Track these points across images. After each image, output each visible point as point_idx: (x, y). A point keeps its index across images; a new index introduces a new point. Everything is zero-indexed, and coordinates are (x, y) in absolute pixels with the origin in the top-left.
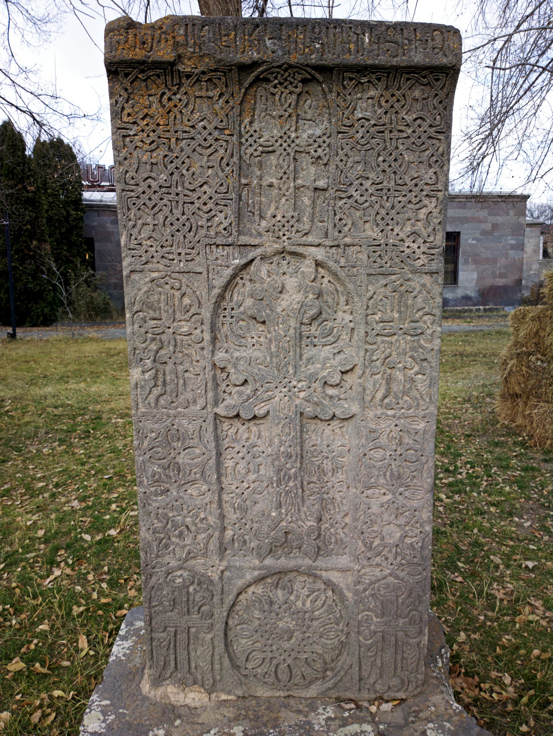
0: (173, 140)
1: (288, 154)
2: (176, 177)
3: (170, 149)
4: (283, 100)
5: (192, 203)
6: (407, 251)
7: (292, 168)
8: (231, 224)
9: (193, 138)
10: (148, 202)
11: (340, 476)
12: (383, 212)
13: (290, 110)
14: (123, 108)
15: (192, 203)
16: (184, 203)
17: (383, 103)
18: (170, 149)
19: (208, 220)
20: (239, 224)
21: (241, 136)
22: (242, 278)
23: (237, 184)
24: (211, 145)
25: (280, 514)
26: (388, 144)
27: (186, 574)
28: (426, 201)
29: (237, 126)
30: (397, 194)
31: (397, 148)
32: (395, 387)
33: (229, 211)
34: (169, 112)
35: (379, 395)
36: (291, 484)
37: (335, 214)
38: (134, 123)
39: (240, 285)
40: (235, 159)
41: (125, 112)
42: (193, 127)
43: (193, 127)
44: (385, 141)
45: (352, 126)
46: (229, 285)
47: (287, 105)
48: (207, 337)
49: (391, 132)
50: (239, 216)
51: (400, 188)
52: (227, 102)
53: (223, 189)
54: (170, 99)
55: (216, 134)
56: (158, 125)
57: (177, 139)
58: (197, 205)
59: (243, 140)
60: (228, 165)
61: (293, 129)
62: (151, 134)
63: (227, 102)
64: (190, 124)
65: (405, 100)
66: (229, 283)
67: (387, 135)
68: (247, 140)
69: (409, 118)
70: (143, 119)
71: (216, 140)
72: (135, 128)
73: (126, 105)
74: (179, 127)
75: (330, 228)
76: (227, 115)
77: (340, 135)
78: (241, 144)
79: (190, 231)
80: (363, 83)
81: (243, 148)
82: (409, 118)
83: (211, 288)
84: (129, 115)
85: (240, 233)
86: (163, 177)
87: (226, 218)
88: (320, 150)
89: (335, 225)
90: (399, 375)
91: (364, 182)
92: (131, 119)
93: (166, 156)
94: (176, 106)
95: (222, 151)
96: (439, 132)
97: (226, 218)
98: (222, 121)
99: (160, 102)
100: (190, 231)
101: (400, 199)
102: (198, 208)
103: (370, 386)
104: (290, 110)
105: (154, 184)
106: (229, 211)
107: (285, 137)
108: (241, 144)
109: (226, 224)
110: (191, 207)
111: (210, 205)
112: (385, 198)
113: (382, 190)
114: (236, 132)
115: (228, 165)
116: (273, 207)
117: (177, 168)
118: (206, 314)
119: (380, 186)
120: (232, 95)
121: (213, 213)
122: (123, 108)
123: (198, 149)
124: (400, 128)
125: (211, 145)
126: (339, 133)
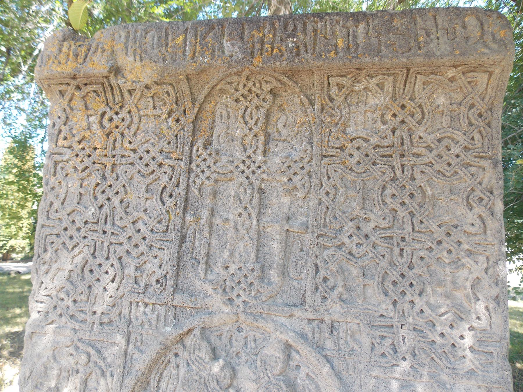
0: (109, 167)
1: (252, 183)
3: (104, 177)
4: (247, 118)
5: (121, 244)
6: (439, 340)
7: (255, 202)
8: (166, 275)
9: (132, 164)
10: (68, 242)
13: (256, 130)
14: (60, 131)
15: (121, 244)
16: (111, 243)
17: (388, 117)
18: (104, 177)
19: (137, 268)
20: (177, 275)
21: (191, 161)
22: (176, 355)
23: (179, 222)
24: (153, 172)
26: (399, 173)
28: (466, 260)
29: (187, 148)
30: (417, 246)
31: (413, 178)
34: (108, 135)
37: (317, 271)
38: (70, 147)
39: (173, 365)
40: (181, 190)
41: (62, 136)
42: (134, 150)
43: (134, 150)
44: (393, 168)
45: (342, 148)
49: (402, 156)
51: (419, 236)
52: (178, 120)
53: (162, 227)
54: (111, 120)
55: (160, 159)
56: (95, 149)
57: (113, 165)
58: (126, 247)
59: (193, 166)
60: (171, 196)
61: (259, 151)
62: (86, 160)
63: (178, 120)
64: (132, 147)
65: (423, 112)
66: (154, 362)
67: (396, 162)
68: (198, 166)
70: (79, 142)
71: (160, 165)
72: (69, 151)
73: (63, 128)
74: (118, 152)
75: (310, 289)
76: (176, 136)
77: (325, 160)
78: (190, 171)
79: (113, 281)
80: (358, 93)
81: (192, 176)
84: (65, 138)
85: (176, 288)
87: (160, 266)
88: (296, 179)
89: (317, 288)
91: (362, 225)
92: (66, 143)
93: (98, 184)
94: (117, 127)
95: (165, 179)
96: (481, 157)
97: (160, 266)
98: (169, 143)
99: (101, 123)
100: (113, 281)
101: (422, 253)
102: (128, 252)
104: (256, 130)
105: (77, 218)
107: (248, 162)
109: (159, 273)
110: (119, 249)
111: (142, 248)
112: (397, 251)
113: (392, 238)
114: (186, 155)
115: (171, 196)
116: (226, 254)
117: (109, 199)
119: (388, 233)
120: (185, 112)
121: (145, 258)
122: (60, 131)
124: (415, 150)
125: (153, 172)
126: (323, 156)
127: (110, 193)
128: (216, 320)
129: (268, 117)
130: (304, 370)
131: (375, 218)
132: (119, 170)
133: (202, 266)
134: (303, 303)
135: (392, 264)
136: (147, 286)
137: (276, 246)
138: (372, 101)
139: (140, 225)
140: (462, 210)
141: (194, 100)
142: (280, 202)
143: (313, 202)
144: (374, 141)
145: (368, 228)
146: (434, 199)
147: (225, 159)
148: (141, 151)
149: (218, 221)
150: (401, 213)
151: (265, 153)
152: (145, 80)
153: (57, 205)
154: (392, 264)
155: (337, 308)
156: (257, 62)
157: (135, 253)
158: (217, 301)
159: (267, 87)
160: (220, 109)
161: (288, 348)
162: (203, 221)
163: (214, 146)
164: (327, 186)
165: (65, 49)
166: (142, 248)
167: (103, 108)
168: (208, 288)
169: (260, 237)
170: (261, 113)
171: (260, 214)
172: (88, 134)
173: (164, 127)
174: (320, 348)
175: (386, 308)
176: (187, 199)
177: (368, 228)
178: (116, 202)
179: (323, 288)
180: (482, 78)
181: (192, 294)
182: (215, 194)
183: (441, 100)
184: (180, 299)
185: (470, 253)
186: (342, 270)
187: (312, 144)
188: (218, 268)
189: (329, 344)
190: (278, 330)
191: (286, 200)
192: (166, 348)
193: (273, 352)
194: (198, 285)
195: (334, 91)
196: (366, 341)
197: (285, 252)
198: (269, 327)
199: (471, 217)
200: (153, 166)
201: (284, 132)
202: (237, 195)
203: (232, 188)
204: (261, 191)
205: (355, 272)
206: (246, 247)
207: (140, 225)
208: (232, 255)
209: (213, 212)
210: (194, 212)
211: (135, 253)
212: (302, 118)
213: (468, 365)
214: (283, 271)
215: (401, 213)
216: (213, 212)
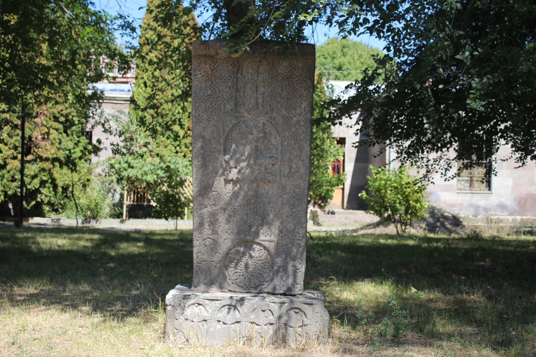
2: (214, 91)
3: (212, 83)
11: (271, 205)
12: (288, 106)
18: (212, 83)
21: (237, 79)
25: (247, 217)
27: (210, 240)
28: (304, 103)
32: (292, 170)
33: (232, 103)
34: (212, 70)
35: (286, 173)
36: (252, 207)
40: (235, 86)
46: (231, 130)
47: (254, 69)
48: (222, 148)
50: (236, 105)
54: (213, 66)
66: (231, 130)
69: (297, 74)
72: (200, 75)
78: (237, 81)
82: (297, 74)
83: (224, 131)
85: (236, 112)
86: (209, 92)
90: (294, 166)
103: (283, 169)
105: (205, 94)
106: (232, 103)
108: (237, 81)
109: (231, 108)
111: (225, 102)
118: (222, 140)
123: (222, 83)
127: (215, 87)
128: (246, 119)
129: (258, 67)
130: (268, 129)
131: (284, 94)
132: (217, 81)
133: (242, 106)
134: (267, 113)
135: (288, 104)
136: (227, 112)
137: (260, 101)
138: (284, 64)
139: (224, 96)
140: (303, 91)
141: (238, 62)
142: (262, 90)
143: (269, 90)
144: (285, 74)
145: (282, 96)
146: (298, 89)
147: (246, 78)
148: (223, 76)
149: (245, 95)
150: (290, 92)
151: (257, 77)
152: (225, 56)
153: (198, 91)
154: (288, 104)
155: (275, 114)
156: (256, 55)
157: (223, 103)
158: (246, 114)
159: (258, 60)
160: (245, 65)
161: (264, 124)
162: (242, 94)
163: (243, 75)
164: (273, 86)
165: (202, 47)
166: (225, 102)
167: (211, 63)
168: (244, 111)
169: (257, 99)
170: (256, 66)
171: (257, 93)
172: (206, 70)
173: (229, 69)
174: (271, 123)
175: (286, 113)
176: (237, 89)
177: (282, 96)
178: (217, 90)
179: (272, 110)
180: (308, 61)
181: (240, 113)
182: (244, 87)
183: (300, 65)
184: (237, 114)
185: (304, 101)
186: (276, 106)
187: (269, 75)
188: (246, 106)
189: (273, 122)
190: (263, 120)
191: (263, 89)
192: (233, 126)
193: (260, 125)
194: (241, 111)
195: (275, 62)
196: (281, 121)
197: (263, 102)
198: (259, 119)
199: (305, 93)
200: (227, 80)
201: (262, 71)
202: (250, 88)
203: (249, 86)
204: (257, 87)
205: (279, 106)
206: (253, 101)
207: (224, 96)
208: (250, 103)
209: (244, 92)
210: (239, 93)
211: (223, 103)
212: (266, 68)
213: (302, 124)
214: (263, 106)
215: (290, 92)
216: (244, 92)
